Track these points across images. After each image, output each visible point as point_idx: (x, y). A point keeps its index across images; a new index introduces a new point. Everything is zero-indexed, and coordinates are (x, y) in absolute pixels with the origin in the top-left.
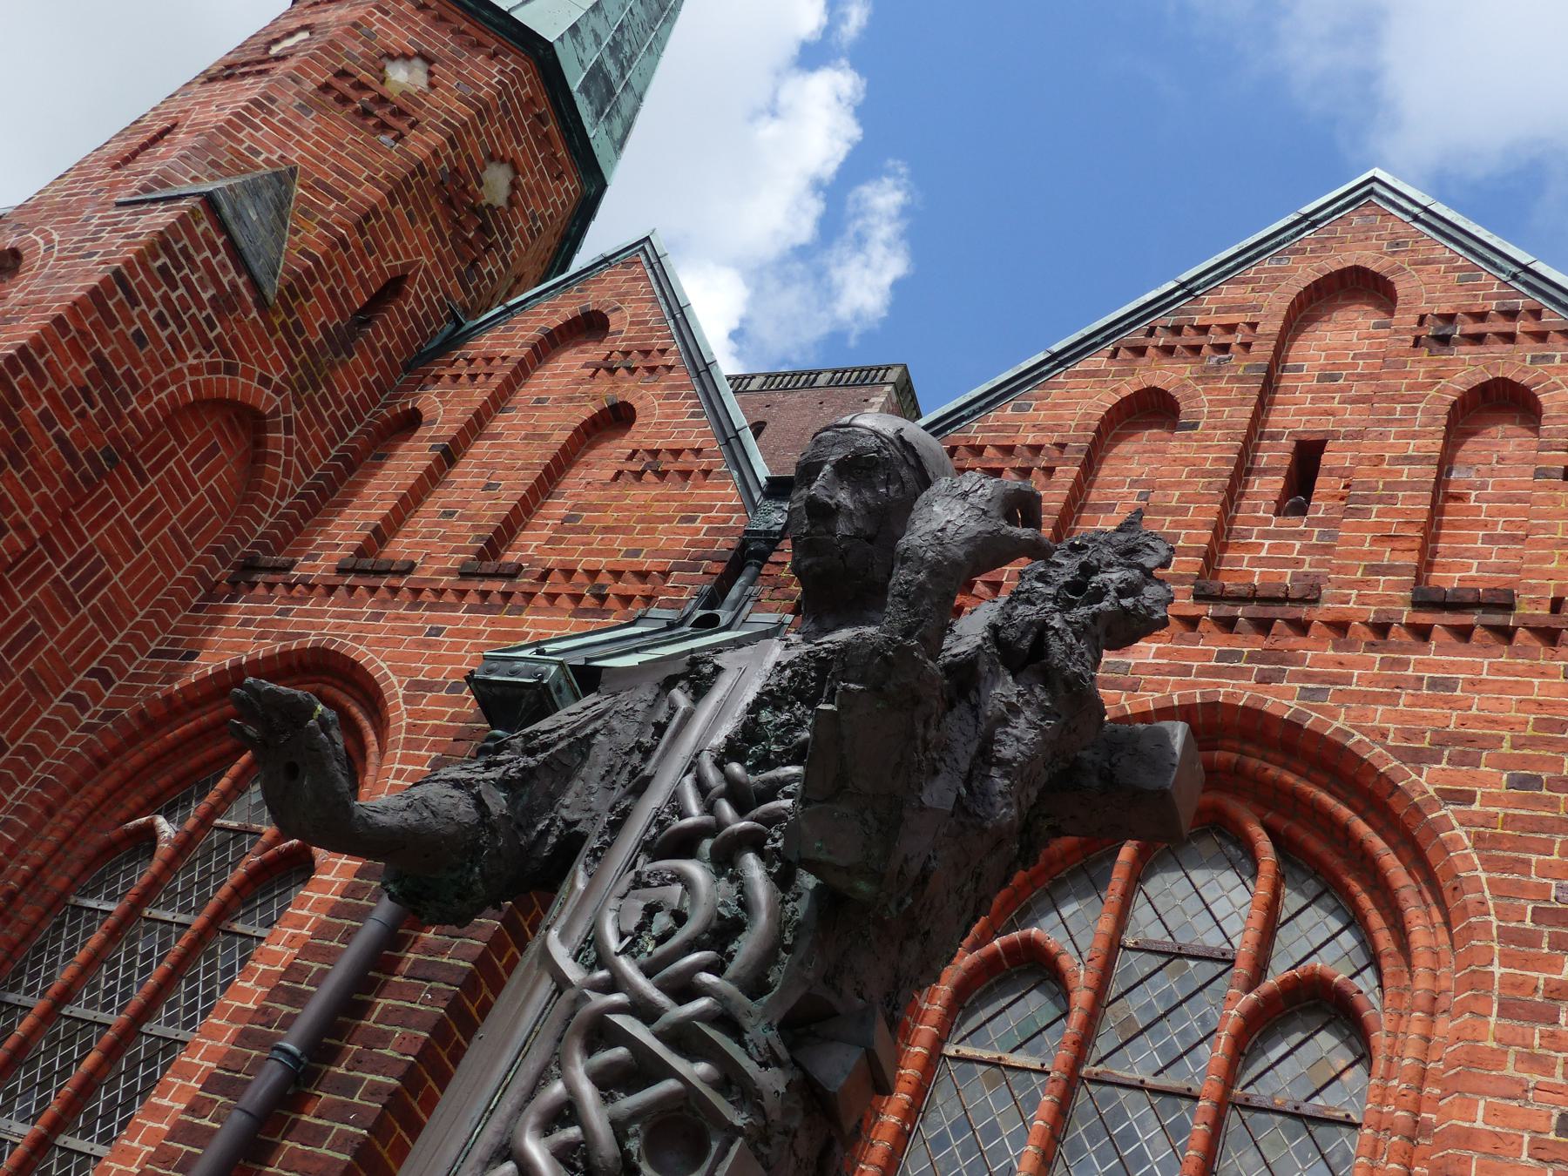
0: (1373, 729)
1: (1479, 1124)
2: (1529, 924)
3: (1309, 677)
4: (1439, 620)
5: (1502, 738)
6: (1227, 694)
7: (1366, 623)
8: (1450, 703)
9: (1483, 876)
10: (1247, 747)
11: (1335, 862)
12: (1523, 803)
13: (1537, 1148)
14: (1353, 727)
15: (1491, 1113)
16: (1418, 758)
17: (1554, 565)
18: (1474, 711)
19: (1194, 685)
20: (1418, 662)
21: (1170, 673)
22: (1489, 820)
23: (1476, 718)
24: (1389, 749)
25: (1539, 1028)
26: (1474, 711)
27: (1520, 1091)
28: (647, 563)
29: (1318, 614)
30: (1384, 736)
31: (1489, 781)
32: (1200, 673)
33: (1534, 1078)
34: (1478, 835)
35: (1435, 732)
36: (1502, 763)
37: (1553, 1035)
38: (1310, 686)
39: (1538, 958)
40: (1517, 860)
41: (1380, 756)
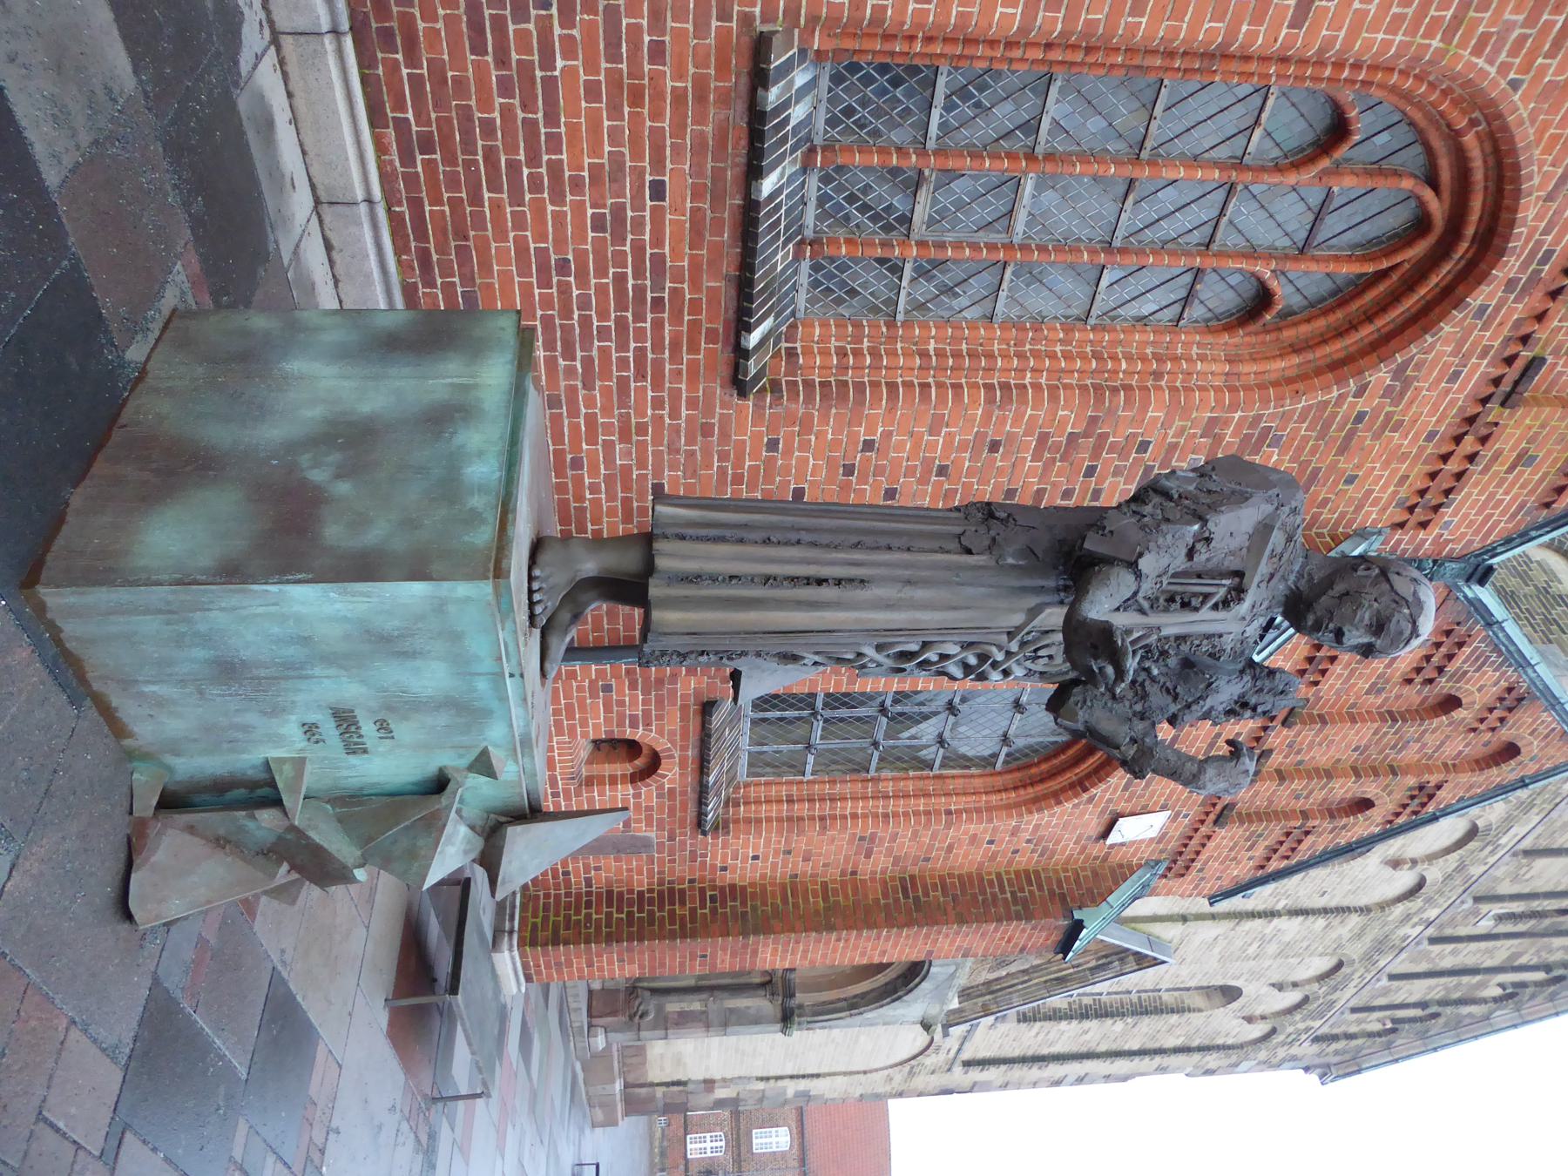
4: (1513, 373)
10: (1463, 262)
11: (1355, 306)
13: (1135, 435)
33: (1171, 432)
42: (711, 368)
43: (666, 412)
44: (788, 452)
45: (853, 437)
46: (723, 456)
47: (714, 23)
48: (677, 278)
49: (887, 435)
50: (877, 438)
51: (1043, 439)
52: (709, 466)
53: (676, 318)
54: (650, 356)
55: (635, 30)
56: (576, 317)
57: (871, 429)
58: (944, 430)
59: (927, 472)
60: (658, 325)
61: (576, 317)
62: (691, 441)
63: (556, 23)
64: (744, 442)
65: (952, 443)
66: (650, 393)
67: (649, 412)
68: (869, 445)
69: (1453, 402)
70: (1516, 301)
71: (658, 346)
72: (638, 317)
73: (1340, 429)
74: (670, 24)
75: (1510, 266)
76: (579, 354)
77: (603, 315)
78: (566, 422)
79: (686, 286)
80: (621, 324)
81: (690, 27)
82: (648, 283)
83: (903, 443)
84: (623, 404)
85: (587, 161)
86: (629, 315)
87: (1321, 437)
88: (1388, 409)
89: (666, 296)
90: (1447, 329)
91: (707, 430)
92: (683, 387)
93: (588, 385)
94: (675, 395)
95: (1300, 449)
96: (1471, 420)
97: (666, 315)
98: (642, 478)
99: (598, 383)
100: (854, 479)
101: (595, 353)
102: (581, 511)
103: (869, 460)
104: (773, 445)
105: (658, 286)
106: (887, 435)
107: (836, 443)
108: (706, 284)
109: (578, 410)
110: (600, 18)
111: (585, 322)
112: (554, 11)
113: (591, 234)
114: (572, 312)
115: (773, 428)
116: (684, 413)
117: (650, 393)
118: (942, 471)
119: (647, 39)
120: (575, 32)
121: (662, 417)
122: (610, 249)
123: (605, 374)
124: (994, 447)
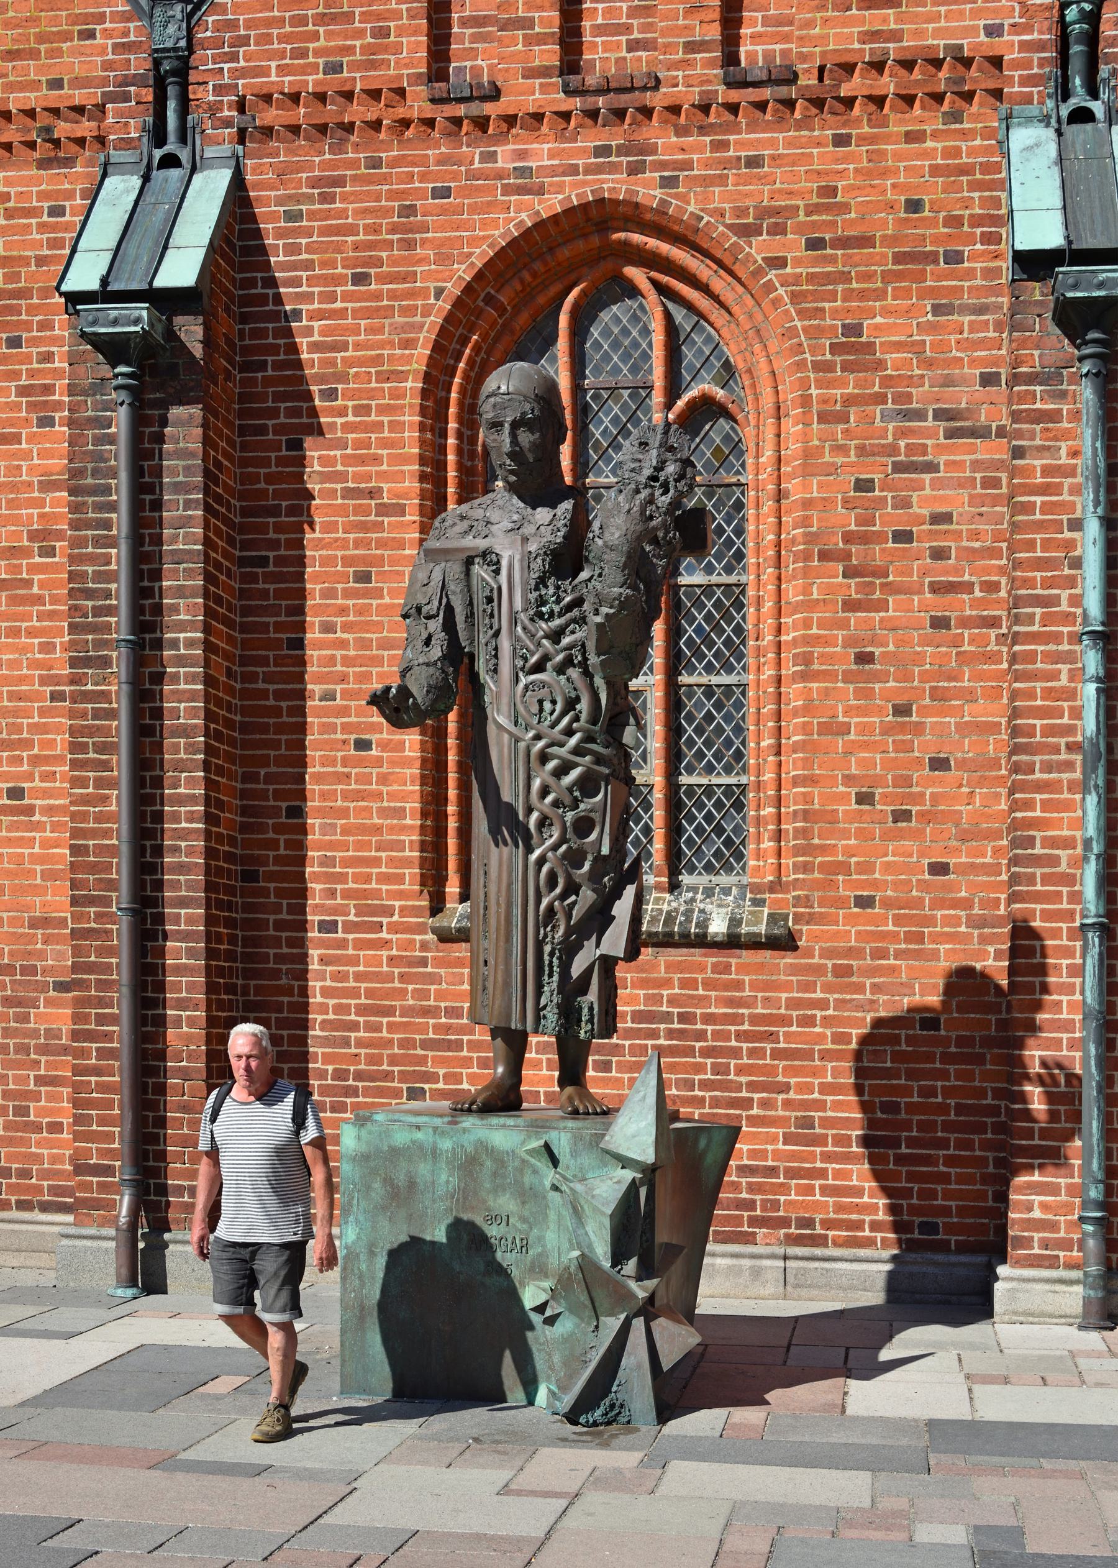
0: (716, 210)
1: (815, 494)
2: (828, 356)
3: (662, 165)
5: (798, 207)
6: (610, 190)
7: (693, 105)
8: (760, 178)
9: (799, 324)
12: (816, 262)
13: (845, 501)
14: (702, 210)
15: (821, 486)
16: (748, 231)
17: (817, 30)
18: (778, 185)
19: (585, 183)
20: (736, 142)
21: (564, 174)
22: (797, 279)
23: (780, 191)
24: (729, 227)
25: (840, 427)
26: (778, 185)
27: (832, 469)
28: (78, 96)
29: (657, 100)
30: (723, 215)
31: (793, 245)
32: (587, 172)
33: (839, 460)
34: (792, 292)
35: (755, 207)
36: (800, 229)
37: (847, 430)
38: (666, 174)
39: (836, 379)
40: (817, 309)
41: (723, 234)
42: (760, 968)
43: (819, 1014)
44: (875, 884)
45: (851, 817)
46: (881, 954)
47: (429, 969)
48: (658, 1000)
49: (848, 780)
50: (853, 791)
51: (851, 606)
52: (893, 970)
53: (703, 1001)
54: (746, 1027)
55: (437, 1028)
56: (701, 1094)
57: (843, 798)
58: (841, 719)
59: (902, 728)
60: (709, 1019)
61: (701, 1094)
62: (860, 988)
63: (434, 1086)
64: (858, 933)
65: (858, 707)
66: (794, 1028)
67: (818, 1030)
68: (864, 798)
69: (789, 144)
70: (653, 150)
71: (736, 1019)
72: (701, 1035)
73: (833, 260)
74: (432, 1003)
75: (615, 185)
76: (744, 1094)
77: (699, 1068)
78: (830, 1114)
79: (665, 993)
80: (707, 1052)
81: (433, 987)
82: (662, 1026)
83: (861, 763)
84: (808, 1055)
85: (545, 1072)
86: (698, 1045)
87: (845, 278)
88: (802, 217)
89: (676, 1010)
90: (691, 208)
91: (843, 971)
92: (784, 996)
93: (785, 1088)
94: (793, 1004)
95: (863, 295)
96: (818, 103)
97: (698, 1011)
98: (910, 1040)
99: (780, 1078)
100: (915, 809)
101: (744, 1079)
102: (960, 1109)
103: (884, 796)
104: (864, 902)
105: (667, 1017)
106: (848, 780)
107: (860, 834)
108: (663, 974)
109: (815, 1101)
110: (430, 1054)
111: (705, 1085)
112: (426, 1086)
113: (614, 1074)
114: (696, 1096)
115: (841, 903)
116: (819, 995)
117: (794, 1028)
118: (902, 710)
119: (444, 1020)
120: (441, 1072)
121: (824, 1018)
122: (628, 1058)
123: (772, 1070)
124: (864, 658)
